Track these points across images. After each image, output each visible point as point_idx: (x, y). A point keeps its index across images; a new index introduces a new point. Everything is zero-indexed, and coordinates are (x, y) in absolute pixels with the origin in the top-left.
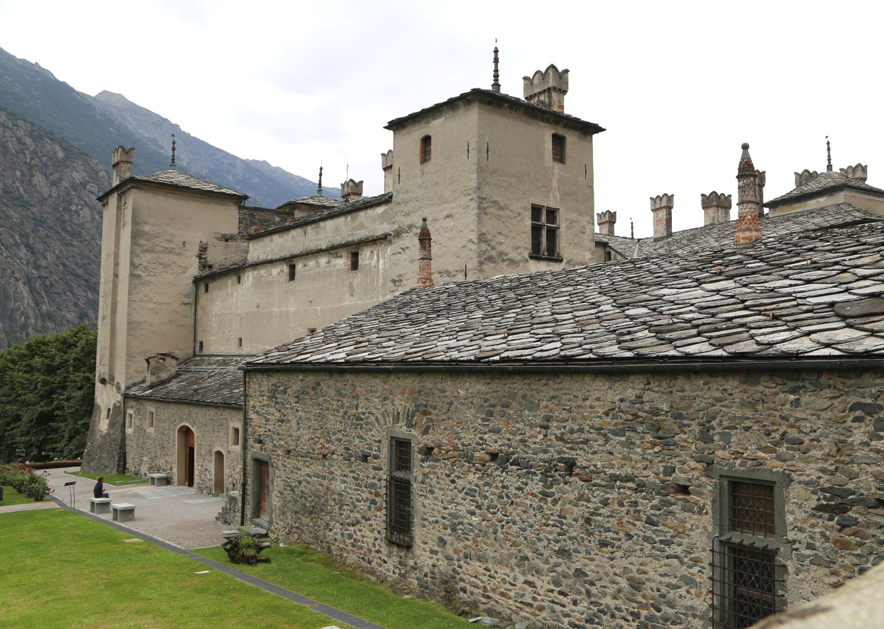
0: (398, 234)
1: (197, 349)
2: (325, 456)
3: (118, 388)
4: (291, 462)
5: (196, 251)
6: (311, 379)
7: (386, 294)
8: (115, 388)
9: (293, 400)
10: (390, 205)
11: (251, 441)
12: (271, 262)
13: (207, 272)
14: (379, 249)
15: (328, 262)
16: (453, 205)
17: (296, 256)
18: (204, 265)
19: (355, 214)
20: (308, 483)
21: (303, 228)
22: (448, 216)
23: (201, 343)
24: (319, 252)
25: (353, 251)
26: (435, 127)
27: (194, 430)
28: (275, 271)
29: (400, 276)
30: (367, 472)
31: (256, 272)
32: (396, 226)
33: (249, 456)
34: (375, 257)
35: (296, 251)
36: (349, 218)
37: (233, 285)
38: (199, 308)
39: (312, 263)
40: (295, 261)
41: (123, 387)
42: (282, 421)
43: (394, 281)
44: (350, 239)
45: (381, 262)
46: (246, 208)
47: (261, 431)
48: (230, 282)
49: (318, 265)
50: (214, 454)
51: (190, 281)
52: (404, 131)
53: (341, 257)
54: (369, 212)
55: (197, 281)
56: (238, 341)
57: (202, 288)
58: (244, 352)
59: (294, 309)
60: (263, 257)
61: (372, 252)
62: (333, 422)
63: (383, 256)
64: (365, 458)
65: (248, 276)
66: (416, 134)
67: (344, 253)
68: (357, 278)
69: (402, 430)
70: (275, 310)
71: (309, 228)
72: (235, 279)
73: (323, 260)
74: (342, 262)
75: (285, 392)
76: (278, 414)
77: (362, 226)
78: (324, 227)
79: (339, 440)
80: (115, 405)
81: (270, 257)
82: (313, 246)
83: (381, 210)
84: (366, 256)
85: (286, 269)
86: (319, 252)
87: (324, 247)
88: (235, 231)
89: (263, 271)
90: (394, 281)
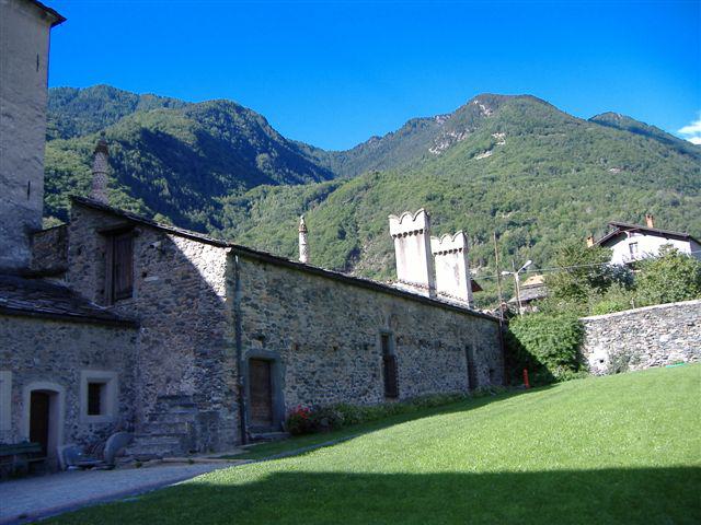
2: (335, 349)
4: (302, 357)
6: (320, 283)
9: (302, 299)
11: (244, 337)
20: (322, 372)
30: (368, 356)
33: (244, 357)
42: (290, 317)
47: (263, 326)
62: (340, 320)
64: (365, 347)
69: (386, 328)
75: (290, 289)
76: (283, 311)
79: (347, 335)
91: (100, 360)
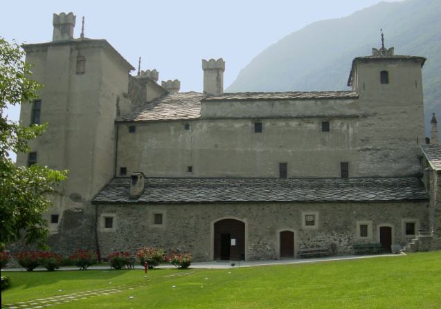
0: (365, 116)
1: (118, 174)
3: (76, 198)
5: (115, 102)
7: (356, 147)
8: (66, 200)
10: (357, 101)
12: (237, 119)
13: (120, 119)
14: (346, 122)
15: (299, 125)
16: (407, 107)
17: (263, 118)
18: (118, 113)
19: (324, 101)
21: (271, 102)
22: (404, 112)
23: (124, 170)
24: (292, 118)
25: (324, 121)
26: (391, 68)
27: (245, 220)
28: (237, 125)
29: (367, 138)
31: (212, 124)
32: (363, 112)
34: (345, 127)
35: (261, 115)
36: (319, 102)
37: (175, 131)
38: (119, 143)
39: (282, 124)
40: (263, 121)
41: (88, 197)
43: (362, 140)
44: (321, 114)
45: (351, 130)
46: (130, 76)
48: (172, 128)
49: (288, 125)
50: (278, 236)
51: (113, 122)
52: (366, 65)
53: (313, 123)
54: (338, 101)
55: (117, 123)
56: (187, 169)
57: (125, 128)
58: (193, 176)
59: (262, 150)
60: (219, 114)
61: (342, 123)
63: (353, 127)
65: (201, 127)
66: (376, 70)
67: (316, 121)
68: (328, 136)
70: (237, 149)
71: (277, 103)
72: (183, 127)
73: (294, 124)
74: (314, 126)
77: (332, 108)
78: (294, 105)
80: (67, 213)
81: (230, 115)
82: (283, 114)
83: (349, 102)
84: (336, 125)
85: (251, 124)
86: (292, 118)
87: (294, 115)
88: (127, 92)
89: (221, 124)
90: (362, 140)
91: (410, 215)
